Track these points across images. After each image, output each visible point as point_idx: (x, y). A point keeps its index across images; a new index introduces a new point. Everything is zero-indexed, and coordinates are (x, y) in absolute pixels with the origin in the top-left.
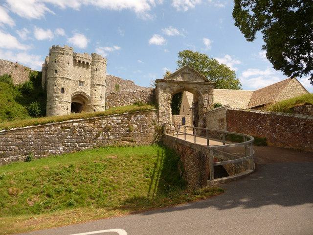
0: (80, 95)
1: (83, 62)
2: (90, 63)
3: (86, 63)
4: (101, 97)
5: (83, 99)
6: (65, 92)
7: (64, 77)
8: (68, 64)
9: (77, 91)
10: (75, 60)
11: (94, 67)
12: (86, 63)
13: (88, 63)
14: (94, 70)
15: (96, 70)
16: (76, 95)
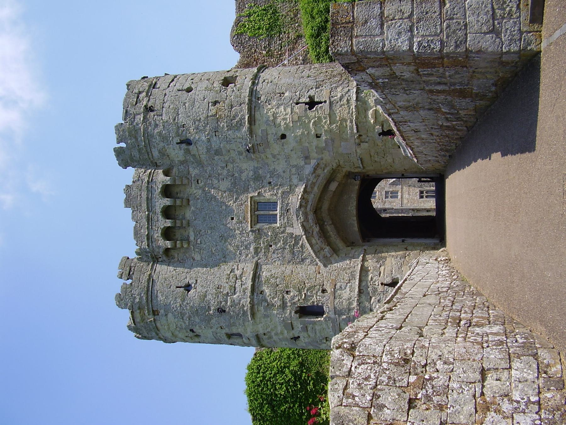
0: (317, 211)
1: (167, 213)
2: (161, 178)
3: (167, 202)
4: (312, 104)
5: (333, 186)
6: (315, 299)
7: (247, 307)
8: (188, 287)
9: (298, 230)
10: (168, 255)
11: (176, 153)
12: (167, 202)
13: (167, 191)
14: (188, 152)
15: (188, 142)
16: (323, 233)
